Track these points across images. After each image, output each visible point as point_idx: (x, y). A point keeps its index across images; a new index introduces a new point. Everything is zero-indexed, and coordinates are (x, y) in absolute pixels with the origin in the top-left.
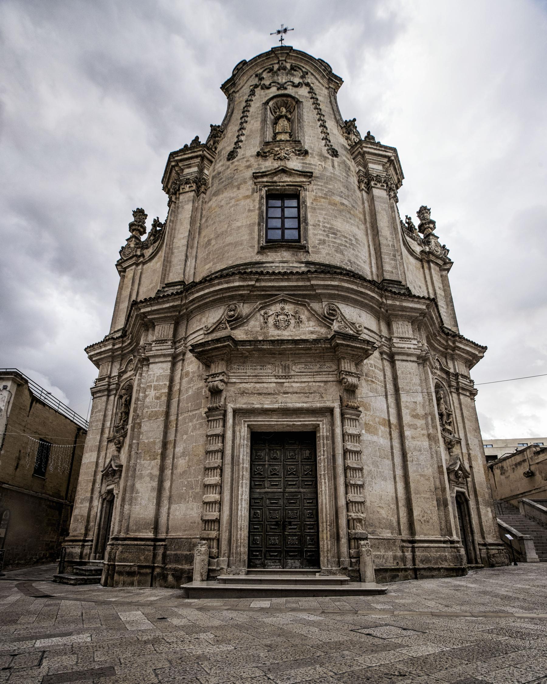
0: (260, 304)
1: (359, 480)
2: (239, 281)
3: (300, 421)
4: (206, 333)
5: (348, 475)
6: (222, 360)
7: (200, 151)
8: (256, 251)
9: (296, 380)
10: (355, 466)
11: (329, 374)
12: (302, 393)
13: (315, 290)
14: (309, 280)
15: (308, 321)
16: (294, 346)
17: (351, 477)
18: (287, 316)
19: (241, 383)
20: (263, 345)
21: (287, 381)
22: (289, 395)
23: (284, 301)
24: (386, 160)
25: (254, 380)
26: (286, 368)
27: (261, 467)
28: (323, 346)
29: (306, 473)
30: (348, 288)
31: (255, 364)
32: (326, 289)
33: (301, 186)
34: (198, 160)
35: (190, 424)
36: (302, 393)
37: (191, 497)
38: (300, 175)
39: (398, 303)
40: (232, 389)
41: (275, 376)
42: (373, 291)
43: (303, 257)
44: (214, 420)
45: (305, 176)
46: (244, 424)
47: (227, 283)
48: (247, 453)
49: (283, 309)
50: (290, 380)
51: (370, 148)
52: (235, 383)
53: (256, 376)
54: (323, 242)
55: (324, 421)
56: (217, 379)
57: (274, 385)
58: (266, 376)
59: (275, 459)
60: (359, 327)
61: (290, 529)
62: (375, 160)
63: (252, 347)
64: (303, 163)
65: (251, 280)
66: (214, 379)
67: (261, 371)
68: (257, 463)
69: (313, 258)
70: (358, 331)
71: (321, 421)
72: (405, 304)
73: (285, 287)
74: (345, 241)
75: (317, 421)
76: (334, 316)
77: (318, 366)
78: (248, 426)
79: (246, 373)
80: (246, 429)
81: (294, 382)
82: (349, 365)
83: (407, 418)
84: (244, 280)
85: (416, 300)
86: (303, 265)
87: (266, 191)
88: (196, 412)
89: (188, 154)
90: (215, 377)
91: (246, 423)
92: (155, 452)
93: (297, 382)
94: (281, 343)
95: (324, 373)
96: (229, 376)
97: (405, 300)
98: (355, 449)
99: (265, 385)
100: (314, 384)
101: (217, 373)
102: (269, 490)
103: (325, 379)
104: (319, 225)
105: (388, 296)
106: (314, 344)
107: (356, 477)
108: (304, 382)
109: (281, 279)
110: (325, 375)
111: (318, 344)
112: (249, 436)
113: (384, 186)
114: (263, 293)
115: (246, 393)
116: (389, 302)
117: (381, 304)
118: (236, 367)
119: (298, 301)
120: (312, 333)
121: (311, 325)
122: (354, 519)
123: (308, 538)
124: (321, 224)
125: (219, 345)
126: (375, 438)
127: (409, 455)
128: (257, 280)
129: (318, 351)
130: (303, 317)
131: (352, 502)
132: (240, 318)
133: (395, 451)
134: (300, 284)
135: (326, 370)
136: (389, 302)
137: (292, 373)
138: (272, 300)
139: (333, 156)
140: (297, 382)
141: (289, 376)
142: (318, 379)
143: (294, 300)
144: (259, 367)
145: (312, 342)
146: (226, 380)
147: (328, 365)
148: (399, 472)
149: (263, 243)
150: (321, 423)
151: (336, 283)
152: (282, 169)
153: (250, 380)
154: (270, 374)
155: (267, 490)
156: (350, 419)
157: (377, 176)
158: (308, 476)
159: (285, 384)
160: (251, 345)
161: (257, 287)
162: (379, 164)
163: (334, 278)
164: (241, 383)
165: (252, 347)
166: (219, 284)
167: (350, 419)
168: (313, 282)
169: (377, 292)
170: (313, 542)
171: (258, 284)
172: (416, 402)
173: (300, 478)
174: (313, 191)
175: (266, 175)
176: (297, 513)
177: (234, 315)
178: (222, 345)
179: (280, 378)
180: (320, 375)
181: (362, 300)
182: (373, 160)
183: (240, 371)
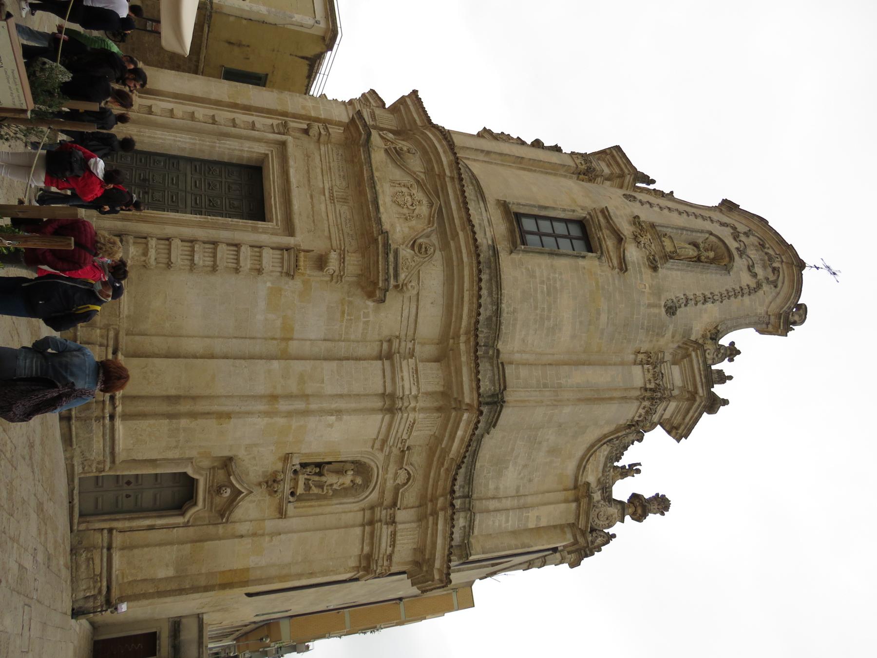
0: (423, 180)
1: (199, 258)
2: (447, 161)
3: (275, 204)
5: (207, 246)
6: (346, 138)
9: (329, 207)
10: (219, 255)
11: (340, 240)
12: (313, 212)
13: (453, 239)
14: (464, 229)
15: (410, 227)
16: (369, 200)
17: (204, 248)
18: (412, 205)
19: (320, 155)
20: (367, 170)
21: (327, 199)
22: (310, 200)
23: (431, 205)
24: (691, 388)
25: (324, 167)
26: (345, 200)
27: (218, 172)
28: (374, 230)
30: (463, 277)
31: (345, 170)
32: (456, 251)
33: (602, 253)
34: (617, 171)
36: (313, 212)
38: (620, 257)
39: (464, 359)
40: (312, 146)
41: (332, 187)
42: (470, 317)
43: (503, 246)
45: (620, 264)
46: (269, 150)
47: (444, 152)
50: (328, 202)
51: (698, 361)
52: (320, 149)
53: (330, 168)
54: (532, 275)
57: (321, 186)
58: (331, 178)
59: (229, 188)
60: (412, 286)
62: (686, 373)
63: (363, 161)
64: (639, 264)
65: (451, 171)
67: (337, 176)
68: (223, 170)
69: (505, 260)
70: (406, 285)
71: (277, 224)
72: (465, 371)
73: (451, 208)
74: (544, 308)
76: (419, 251)
77: (351, 233)
79: (333, 161)
81: (326, 205)
82: (356, 263)
83: (298, 366)
84: (450, 166)
85: (474, 385)
86: (490, 242)
87: (586, 217)
91: (270, 153)
93: (327, 208)
94: (371, 187)
95: (341, 236)
96: (327, 144)
97: (471, 368)
98: (241, 258)
99: (320, 177)
100: (326, 225)
102: (189, 179)
103: (333, 236)
104: (555, 273)
105: (470, 343)
106: (375, 220)
107: (204, 256)
108: (328, 216)
109: (459, 201)
110: (339, 237)
111: (376, 224)
113: (650, 383)
114: (439, 188)
115: (308, 160)
116: (462, 347)
117: (457, 336)
119: (433, 218)
121: (404, 229)
122: (147, 244)
124: (557, 276)
125: (361, 128)
126: (262, 305)
127: (243, 362)
128: (452, 178)
129: (368, 228)
130: (413, 223)
131: (170, 245)
132: (401, 158)
133: (248, 341)
134: (457, 222)
135: (346, 240)
136: (462, 347)
137: (338, 207)
138: (430, 193)
139: (665, 306)
140: (327, 208)
141: (334, 203)
142: (332, 230)
143: (434, 215)
144: (342, 174)
145: (377, 217)
146: (322, 139)
147: (353, 243)
148: (219, 346)
149: (515, 209)
151: (465, 259)
152: (622, 239)
153: (324, 164)
154: (334, 182)
155: (189, 176)
156: (282, 259)
157: (662, 374)
159: (323, 197)
160: (365, 159)
161: (444, 179)
162: (683, 381)
163: (472, 257)
164: (320, 155)
165: (363, 161)
166: (442, 146)
167: (282, 259)
168: (461, 235)
169: (470, 323)
171: (447, 179)
174: (603, 271)
175: (608, 222)
176: (159, 201)
178: (362, 131)
179: (330, 192)
180: (339, 232)
181: (455, 303)
182: (685, 370)
183: (335, 155)
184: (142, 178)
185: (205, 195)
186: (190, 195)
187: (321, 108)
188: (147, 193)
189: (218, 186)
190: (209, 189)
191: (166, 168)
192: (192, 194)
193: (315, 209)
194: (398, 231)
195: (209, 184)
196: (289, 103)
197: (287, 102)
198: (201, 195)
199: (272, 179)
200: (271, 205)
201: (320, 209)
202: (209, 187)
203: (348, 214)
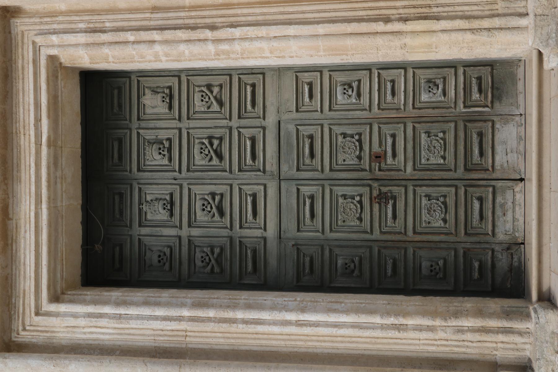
3: (38, 120)
27: (198, 255)
29: (215, 107)
48: (146, 303)
55: (39, 40)
61: (394, 155)
75: (35, 62)
78: (55, 298)
80: (63, 308)
112: (91, 293)
123: (425, 97)
150: (45, 52)
158: (225, 98)
170: (440, 82)
176: (345, 135)
184: (391, 202)
185: (231, 172)
186: (268, 168)
188: (378, 157)
189: (199, 204)
190: (222, 195)
191: (331, 250)
192: (264, 171)
195: (222, 213)
198: (240, 170)
199: (44, 206)
200: (49, 117)
202: (221, 201)
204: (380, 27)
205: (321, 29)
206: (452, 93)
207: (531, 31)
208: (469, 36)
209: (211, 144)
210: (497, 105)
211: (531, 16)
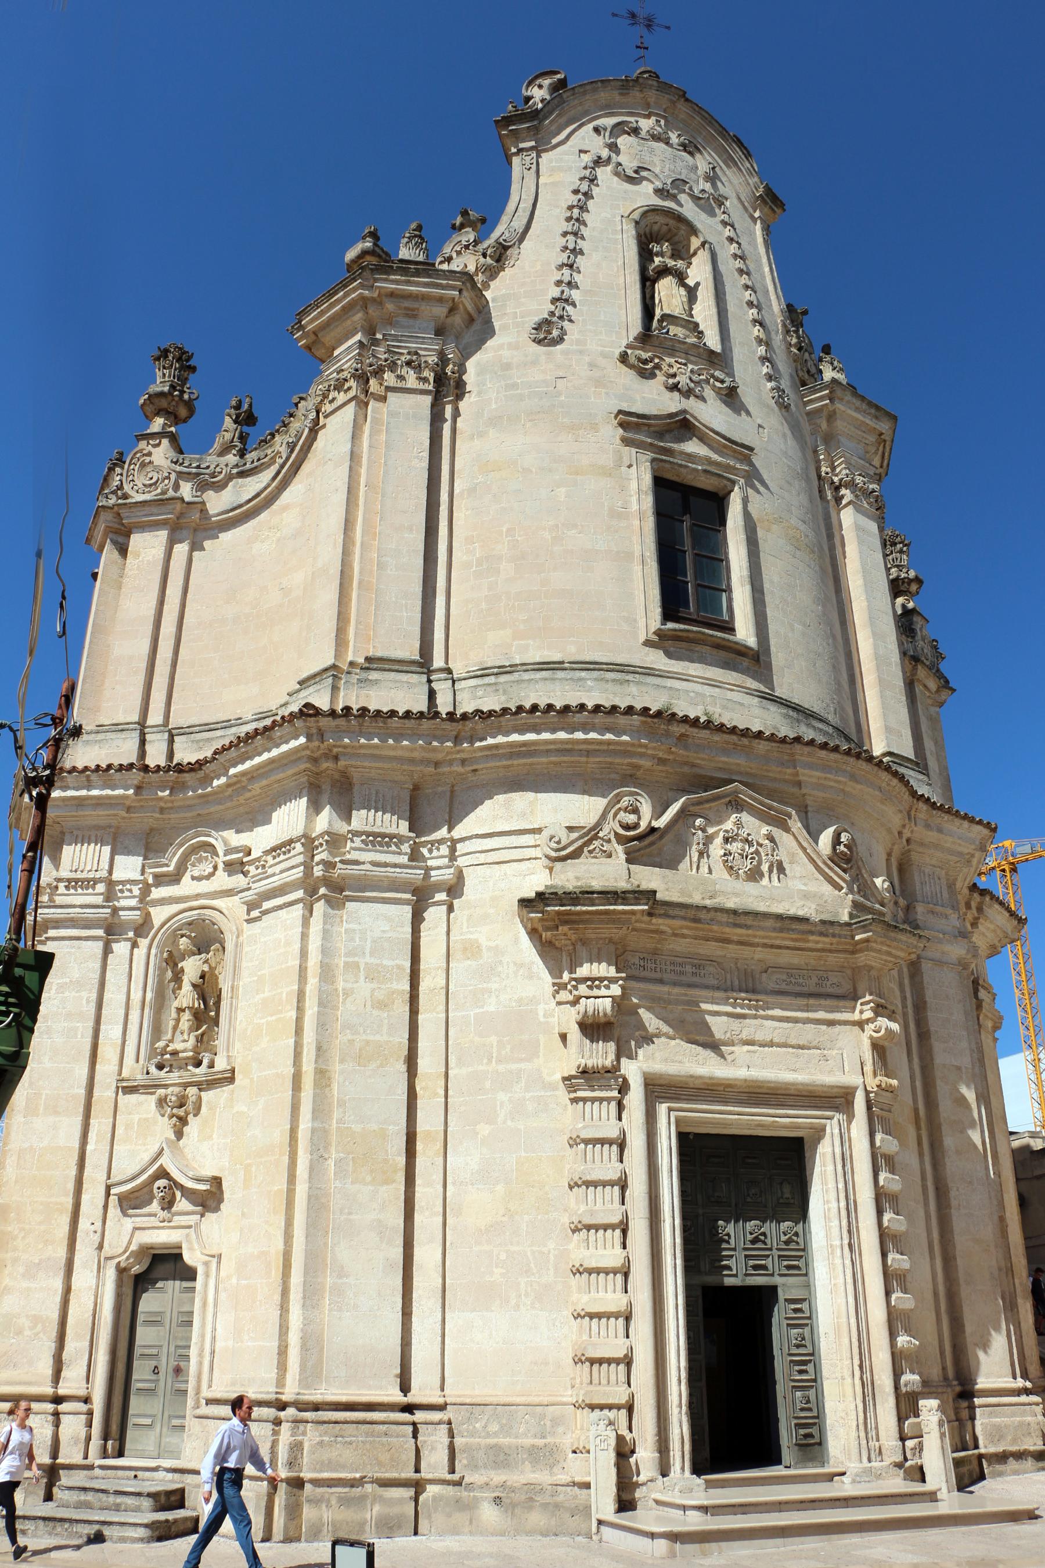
4: (553, 854)
7: (453, 288)
8: (642, 638)
22: (756, 1048)
35: (502, 1096)
37: (527, 1295)
44: (593, 1100)
49: (739, 824)
55: (836, 1119)
56: (603, 992)
66: (596, 992)
78: (678, 1122)
88: (522, 1066)
89: (418, 284)
90: (598, 987)
92: (386, 1161)
101: (605, 979)
118: (637, 962)
120: (806, 896)
123: (798, 1394)
158: (792, 1246)
172: (959, 1068)
173: (775, 1253)
177: (636, 826)
187: (368, 959)
193: (776, 1040)
194: (803, 888)
196: (371, 1038)
197: (368, 1042)
201: (775, 1029)
203: (778, 976)
204: (857, 1362)
205: (853, 1320)
206: (803, 1414)
207: (861, 1465)
208: (855, 1424)
209: (761, 1234)
210: (796, 1448)
211: (869, 1465)
